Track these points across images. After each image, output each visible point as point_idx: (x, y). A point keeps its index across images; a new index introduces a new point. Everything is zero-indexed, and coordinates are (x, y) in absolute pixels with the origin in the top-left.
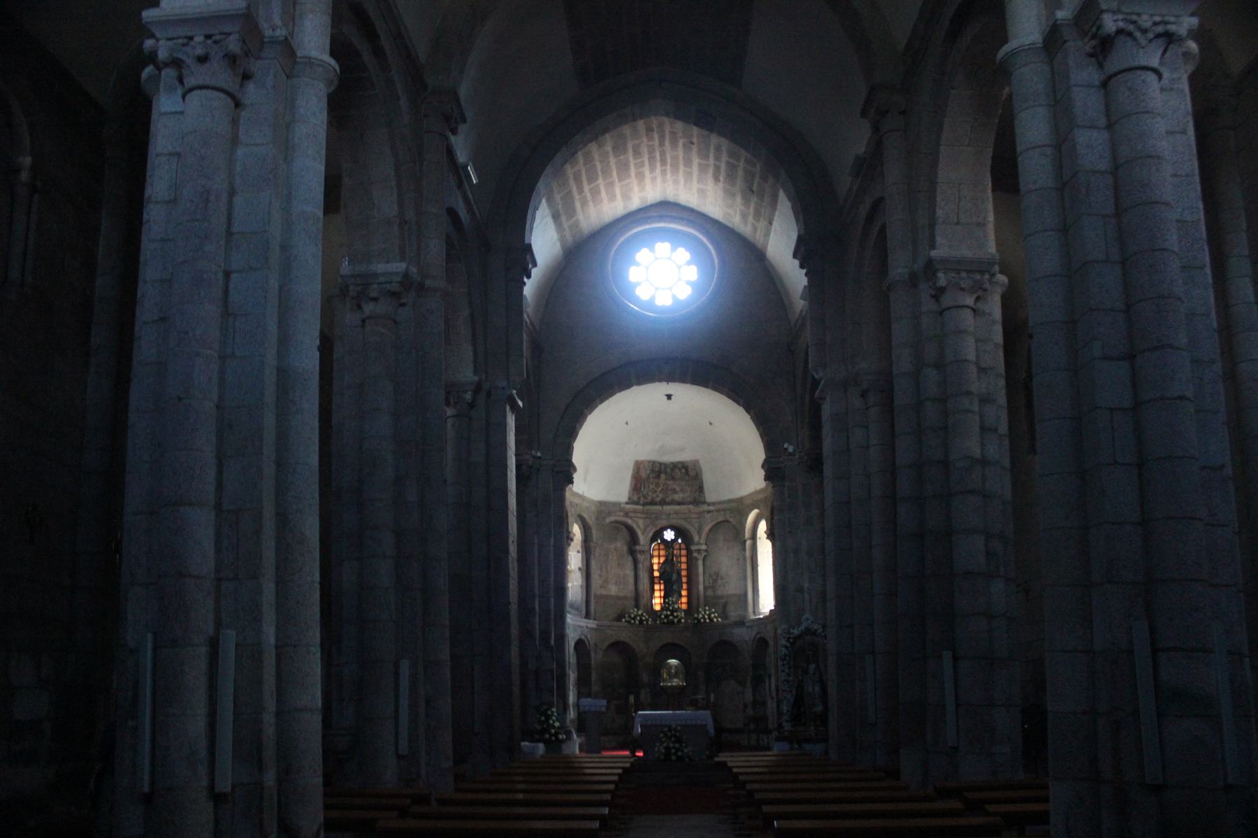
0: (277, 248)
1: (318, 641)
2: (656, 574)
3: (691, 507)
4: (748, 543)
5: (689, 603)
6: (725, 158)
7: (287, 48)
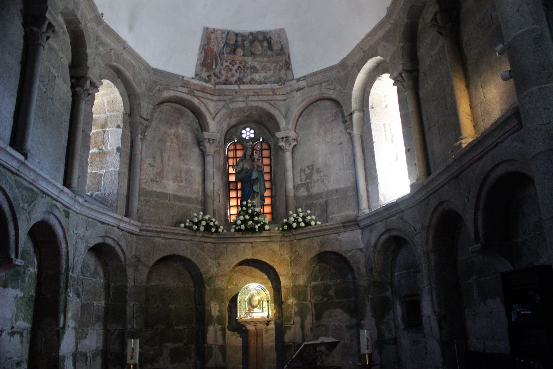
2: (232, 178)
3: (276, 86)
4: (356, 116)
5: (272, 213)
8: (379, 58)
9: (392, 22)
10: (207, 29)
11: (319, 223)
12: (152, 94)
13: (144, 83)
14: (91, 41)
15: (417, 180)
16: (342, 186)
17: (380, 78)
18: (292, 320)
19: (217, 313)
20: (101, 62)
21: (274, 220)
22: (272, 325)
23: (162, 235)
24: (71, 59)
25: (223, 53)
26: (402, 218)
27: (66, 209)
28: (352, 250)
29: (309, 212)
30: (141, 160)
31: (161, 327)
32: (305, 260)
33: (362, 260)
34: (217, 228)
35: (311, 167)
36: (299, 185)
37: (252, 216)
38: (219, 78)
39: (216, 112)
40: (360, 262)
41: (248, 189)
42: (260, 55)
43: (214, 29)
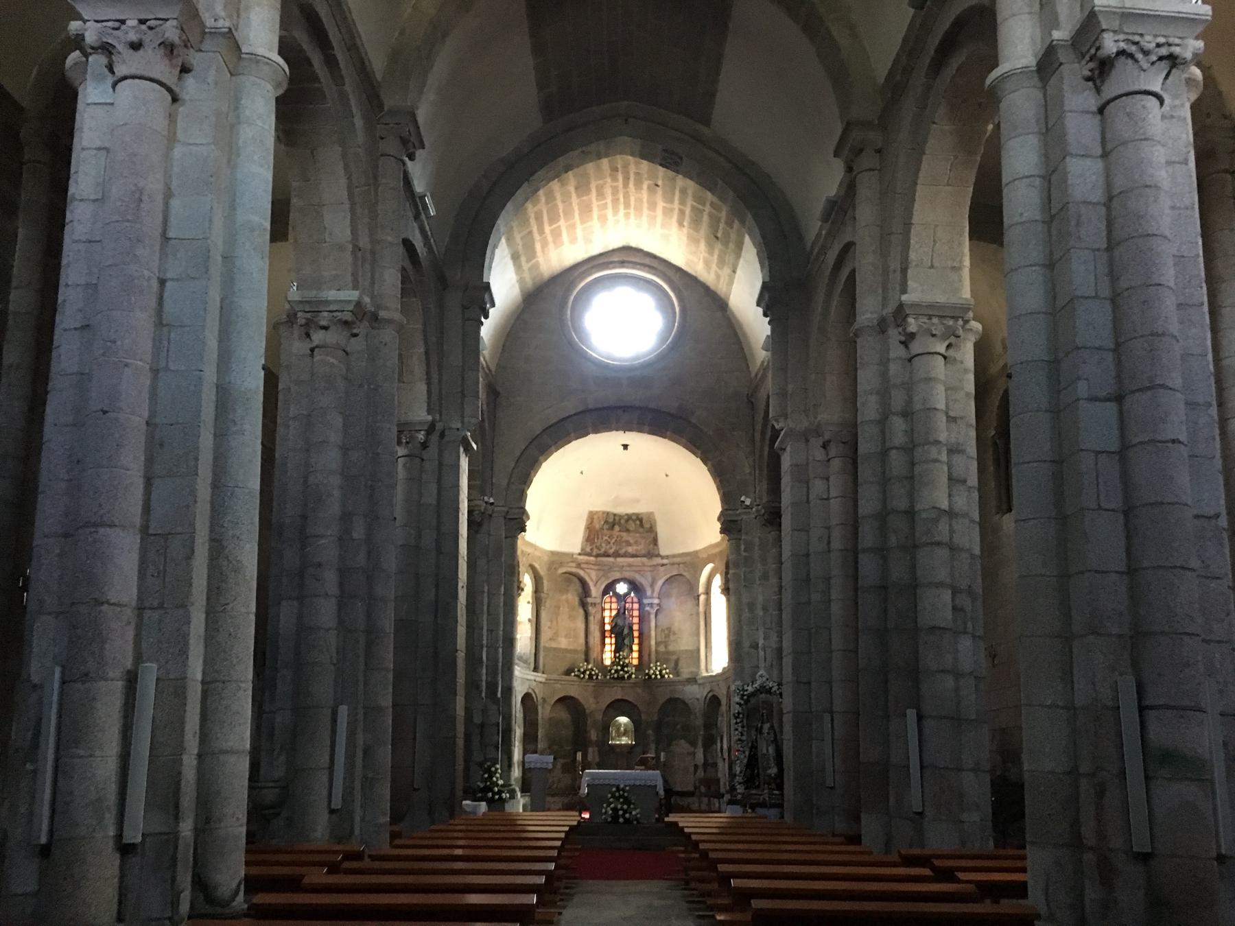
0: (220, 259)
1: (250, 676)
2: (608, 627)
3: (644, 559)
4: (702, 598)
5: (640, 658)
6: (690, 202)
7: (231, 40)
16: (690, 648)
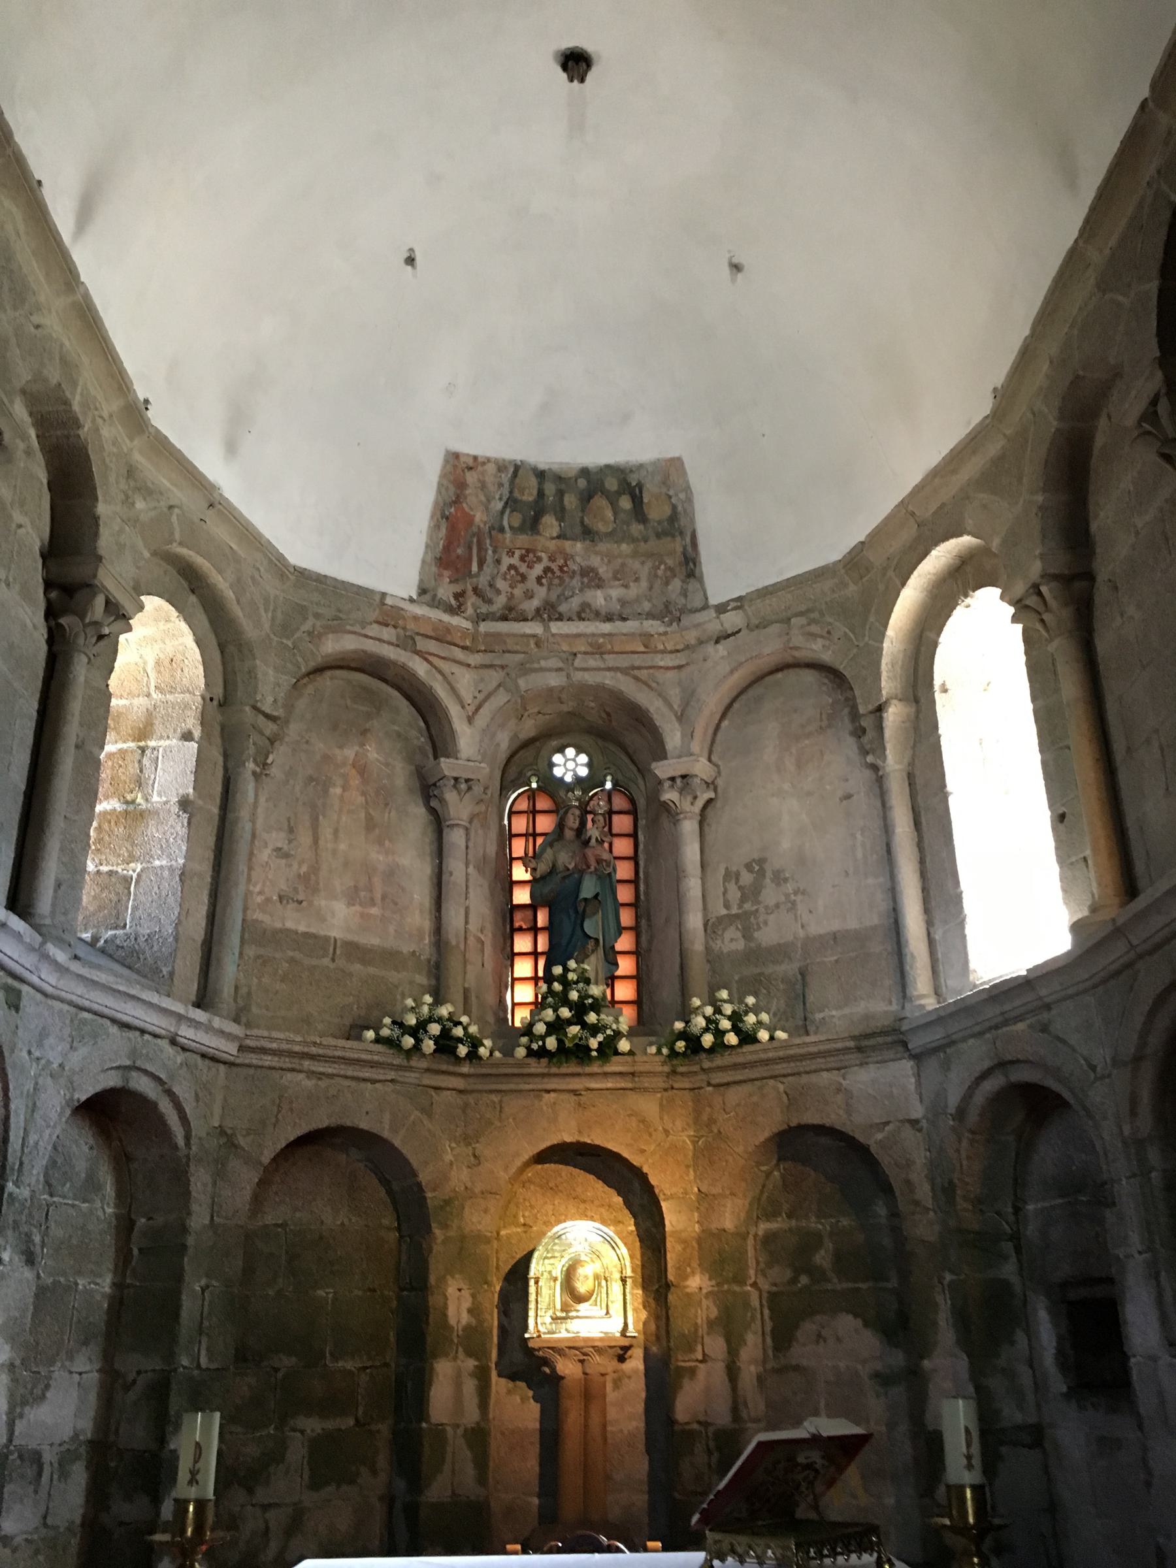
2: (522, 896)
4: (894, 715)
5: (638, 1003)
8: (966, 540)
9: (1008, 432)
10: (457, 456)
11: (781, 1035)
12: (290, 644)
13: (266, 611)
14: (112, 478)
15: (1094, 909)
16: (852, 924)
17: (968, 601)
18: (699, 1348)
19: (465, 1318)
20: (140, 543)
21: (644, 1026)
22: (636, 1363)
23: (306, 1064)
24: (48, 529)
25: (502, 530)
26: (1045, 1028)
27: (10, 981)
28: (888, 1123)
29: (751, 1000)
30: (254, 836)
31: (286, 1362)
32: (740, 1149)
33: (920, 1157)
34: (475, 1043)
35: (757, 866)
36: (720, 920)
37: (580, 1010)
38: (490, 602)
39: (477, 702)
40: (911, 1160)
41: (567, 927)
42: (610, 535)
43: (475, 458)
